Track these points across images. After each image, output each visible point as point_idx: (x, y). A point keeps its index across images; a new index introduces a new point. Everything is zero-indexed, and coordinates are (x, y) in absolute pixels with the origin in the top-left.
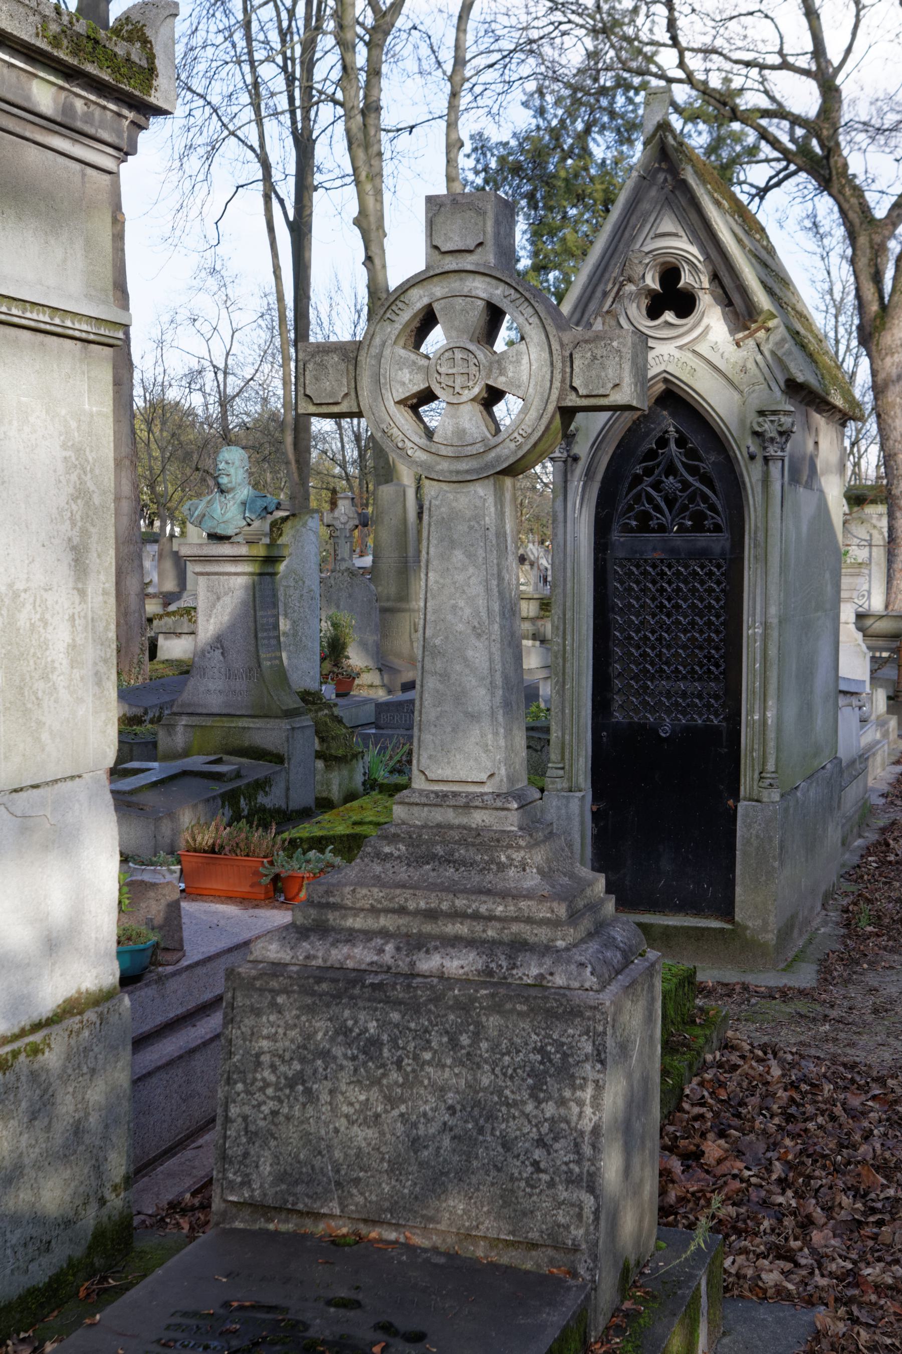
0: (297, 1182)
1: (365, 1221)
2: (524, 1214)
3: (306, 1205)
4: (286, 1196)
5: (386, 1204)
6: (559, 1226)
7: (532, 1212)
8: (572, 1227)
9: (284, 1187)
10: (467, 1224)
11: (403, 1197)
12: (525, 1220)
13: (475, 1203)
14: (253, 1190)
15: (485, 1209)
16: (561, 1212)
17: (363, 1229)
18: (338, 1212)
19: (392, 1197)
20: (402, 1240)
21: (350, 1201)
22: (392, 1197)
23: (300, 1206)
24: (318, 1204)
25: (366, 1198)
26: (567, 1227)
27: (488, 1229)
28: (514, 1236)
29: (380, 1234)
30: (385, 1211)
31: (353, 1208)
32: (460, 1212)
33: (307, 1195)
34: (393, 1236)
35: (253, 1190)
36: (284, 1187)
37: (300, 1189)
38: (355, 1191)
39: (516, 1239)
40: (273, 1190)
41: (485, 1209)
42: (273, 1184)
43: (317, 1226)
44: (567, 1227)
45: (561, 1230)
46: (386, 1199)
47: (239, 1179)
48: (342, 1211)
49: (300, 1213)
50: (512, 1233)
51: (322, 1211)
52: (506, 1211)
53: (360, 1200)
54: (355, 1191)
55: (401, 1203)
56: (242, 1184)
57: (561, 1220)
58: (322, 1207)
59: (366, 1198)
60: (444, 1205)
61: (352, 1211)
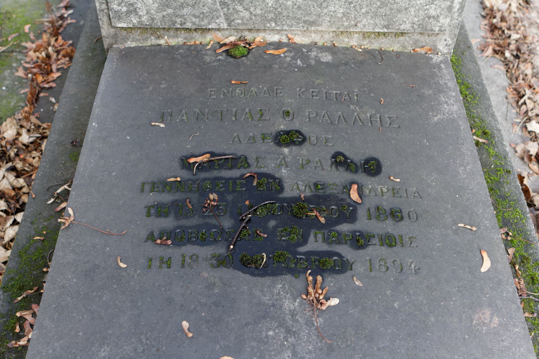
0: (182, 6)
1: (250, 30)
2: (399, 11)
3: (194, 24)
4: (174, 18)
5: (271, 15)
6: (429, 18)
7: (406, 9)
8: (441, 18)
9: (170, 11)
10: (346, 24)
11: (287, 9)
12: (399, 16)
13: (355, 6)
14: (140, 17)
15: (363, 11)
16: (433, 6)
17: (249, 36)
18: (225, 26)
19: (276, 9)
20: (285, 40)
21: (236, 16)
22: (276, 9)
23: (189, 25)
24: (206, 21)
25: (251, 13)
26: (436, 18)
27: (364, 26)
28: (387, 28)
29: (264, 38)
30: (269, 21)
31: (240, 21)
32: (340, 15)
33: (194, 16)
34: (275, 38)
35: (140, 17)
36: (170, 11)
37: (186, 11)
38: (240, 8)
39: (389, 31)
40: (160, 15)
41: (363, 11)
42: (158, 10)
43: (205, 38)
44: (436, 18)
45: (431, 20)
46: (270, 12)
47: (124, 9)
48: (229, 25)
49: (188, 30)
50: (387, 27)
51: (210, 27)
52: (382, 10)
53: (247, 14)
54: (240, 8)
55: (285, 13)
56: (129, 12)
57: (432, 12)
58: (209, 24)
59: (251, 13)
60: (325, 11)
61: (239, 24)
